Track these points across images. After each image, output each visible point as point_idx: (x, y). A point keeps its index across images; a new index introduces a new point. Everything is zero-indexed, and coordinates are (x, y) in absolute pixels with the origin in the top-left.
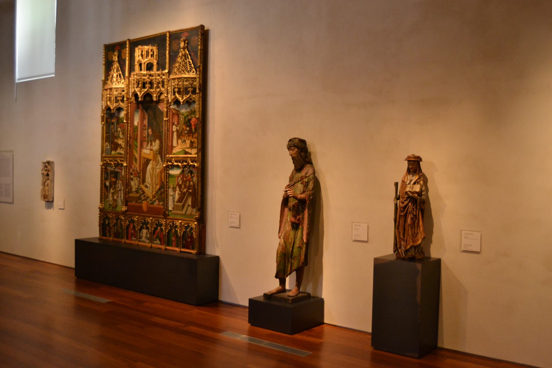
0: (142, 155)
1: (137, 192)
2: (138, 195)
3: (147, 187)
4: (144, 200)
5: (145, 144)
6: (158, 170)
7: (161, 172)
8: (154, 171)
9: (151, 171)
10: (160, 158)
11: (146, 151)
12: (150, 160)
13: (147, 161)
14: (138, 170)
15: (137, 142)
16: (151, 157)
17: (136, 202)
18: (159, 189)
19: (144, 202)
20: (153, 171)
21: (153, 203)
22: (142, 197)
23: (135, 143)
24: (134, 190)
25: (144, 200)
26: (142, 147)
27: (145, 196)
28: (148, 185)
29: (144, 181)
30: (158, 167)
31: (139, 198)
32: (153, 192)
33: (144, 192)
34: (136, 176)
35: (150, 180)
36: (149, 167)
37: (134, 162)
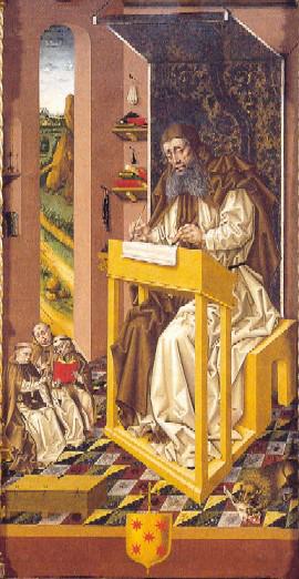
0: (115, 269)
1: (75, 466)
2: (87, 482)
3: (159, 436)
4: (134, 507)
5: (135, 216)
6: (243, 351)
7: (267, 361)
8: (218, 359)
9: (193, 355)
10: (256, 288)
11: (148, 254)
12: (180, 300)
13: (163, 306)
14: (85, 350)
15: (70, 200)
16: (188, 276)
17: (76, 518)
18: (257, 446)
19: (132, 517)
20: (207, 353)
21: (208, 518)
22: (124, 492)
23: (55, 205)
24: (50, 454)
25: (134, 507)
26: (108, 220)
27: (143, 486)
28: (171, 429)
29: (133, 405)
30: (245, 330)
31: (99, 497)
32: (206, 460)
33: (134, 467)
34: (67, 382)
35: (182, 399)
36: (173, 334)
37: (47, 310)
